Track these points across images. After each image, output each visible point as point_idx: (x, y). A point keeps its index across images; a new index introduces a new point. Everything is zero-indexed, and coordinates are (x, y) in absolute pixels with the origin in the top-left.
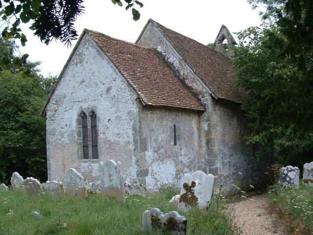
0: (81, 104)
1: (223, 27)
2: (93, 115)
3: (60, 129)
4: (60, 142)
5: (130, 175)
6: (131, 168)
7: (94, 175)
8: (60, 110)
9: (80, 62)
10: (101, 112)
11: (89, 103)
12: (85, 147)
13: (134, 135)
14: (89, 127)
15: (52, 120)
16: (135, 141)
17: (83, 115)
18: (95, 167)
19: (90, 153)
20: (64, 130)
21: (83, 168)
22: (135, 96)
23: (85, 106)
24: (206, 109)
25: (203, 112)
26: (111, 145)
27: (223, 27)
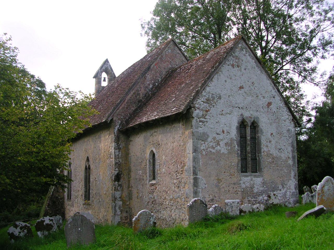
0: (241, 111)
1: (107, 61)
2: (254, 126)
3: (215, 135)
4: (213, 151)
5: (290, 189)
6: (290, 181)
7: (255, 190)
8: (213, 110)
9: (238, 66)
10: (264, 125)
11: (251, 112)
12: (244, 159)
13: (293, 152)
14: (249, 138)
15: (200, 121)
16: (293, 157)
17: (242, 125)
18: (255, 182)
19: (250, 166)
20: (221, 137)
21: (244, 183)
23: (247, 114)
26: (275, 159)
27: (107, 61)
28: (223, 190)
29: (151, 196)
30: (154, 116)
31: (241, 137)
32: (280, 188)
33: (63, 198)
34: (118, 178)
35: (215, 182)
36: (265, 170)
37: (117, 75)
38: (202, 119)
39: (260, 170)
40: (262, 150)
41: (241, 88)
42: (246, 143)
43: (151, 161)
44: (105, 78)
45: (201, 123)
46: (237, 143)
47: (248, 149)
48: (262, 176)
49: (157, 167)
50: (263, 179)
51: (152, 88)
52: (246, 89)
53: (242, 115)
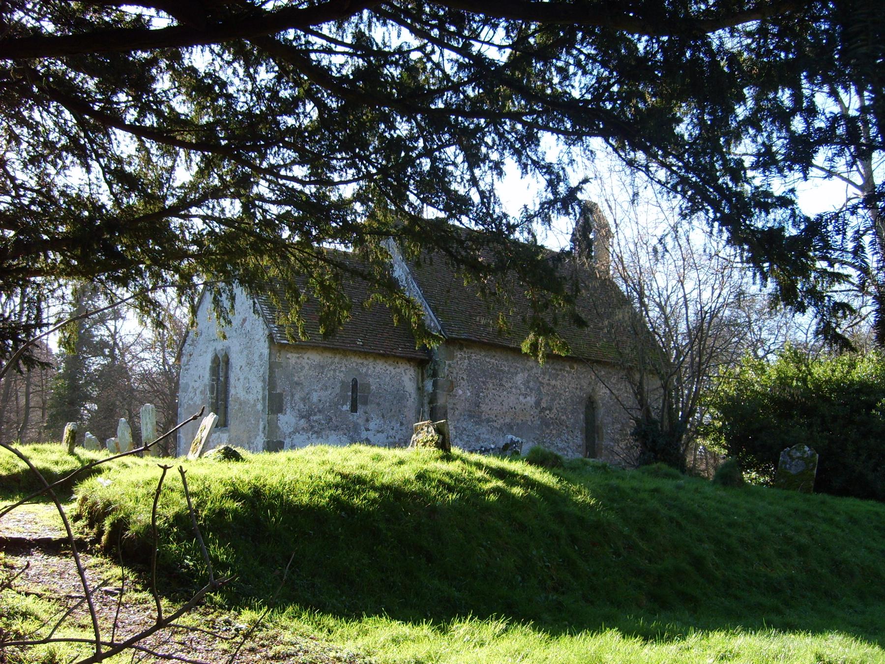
0: (215, 344)
2: (227, 362)
4: (192, 403)
6: (258, 438)
13: (264, 389)
15: (186, 370)
16: (264, 398)
17: (216, 360)
22: (267, 332)
24: (431, 358)
25: (427, 362)
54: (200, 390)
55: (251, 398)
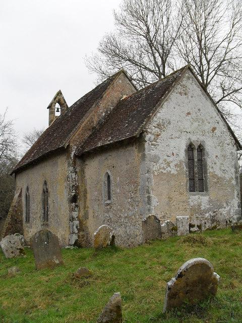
0: (189, 135)
1: (60, 93)
2: (201, 149)
3: (166, 157)
4: (165, 172)
6: (234, 200)
7: (203, 208)
8: (163, 134)
9: (186, 94)
10: (209, 148)
12: (192, 179)
14: (196, 160)
15: (152, 145)
16: (237, 178)
17: (190, 148)
18: (202, 200)
20: (171, 159)
21: (192, 201)
23: (194, 138)
27: (60, 93)
28: (173, 207)
29: (106, 214)
30: (109, 141)
31: (189, 159)
32: (225, 206)
33: (21, 221)
34: (74, 199)
35: (167, 200)
36: (211, 189)
37: (69, 106)
38: (153, 143)
39: (207, 190)
40: (208, 171)
41: (189, 114)
42: (193, 165)
43: (106, 183)
44: (58, 109)
45: (153, 146)
46: (185, 164)
47: (196, 169)
48: (209, 195)
49: (112, 188)
50: (210, 198)
51: (105, 116)
52: (194, 115)
53: (189, 139)
54: (175, 163)
55: (227, 176)
